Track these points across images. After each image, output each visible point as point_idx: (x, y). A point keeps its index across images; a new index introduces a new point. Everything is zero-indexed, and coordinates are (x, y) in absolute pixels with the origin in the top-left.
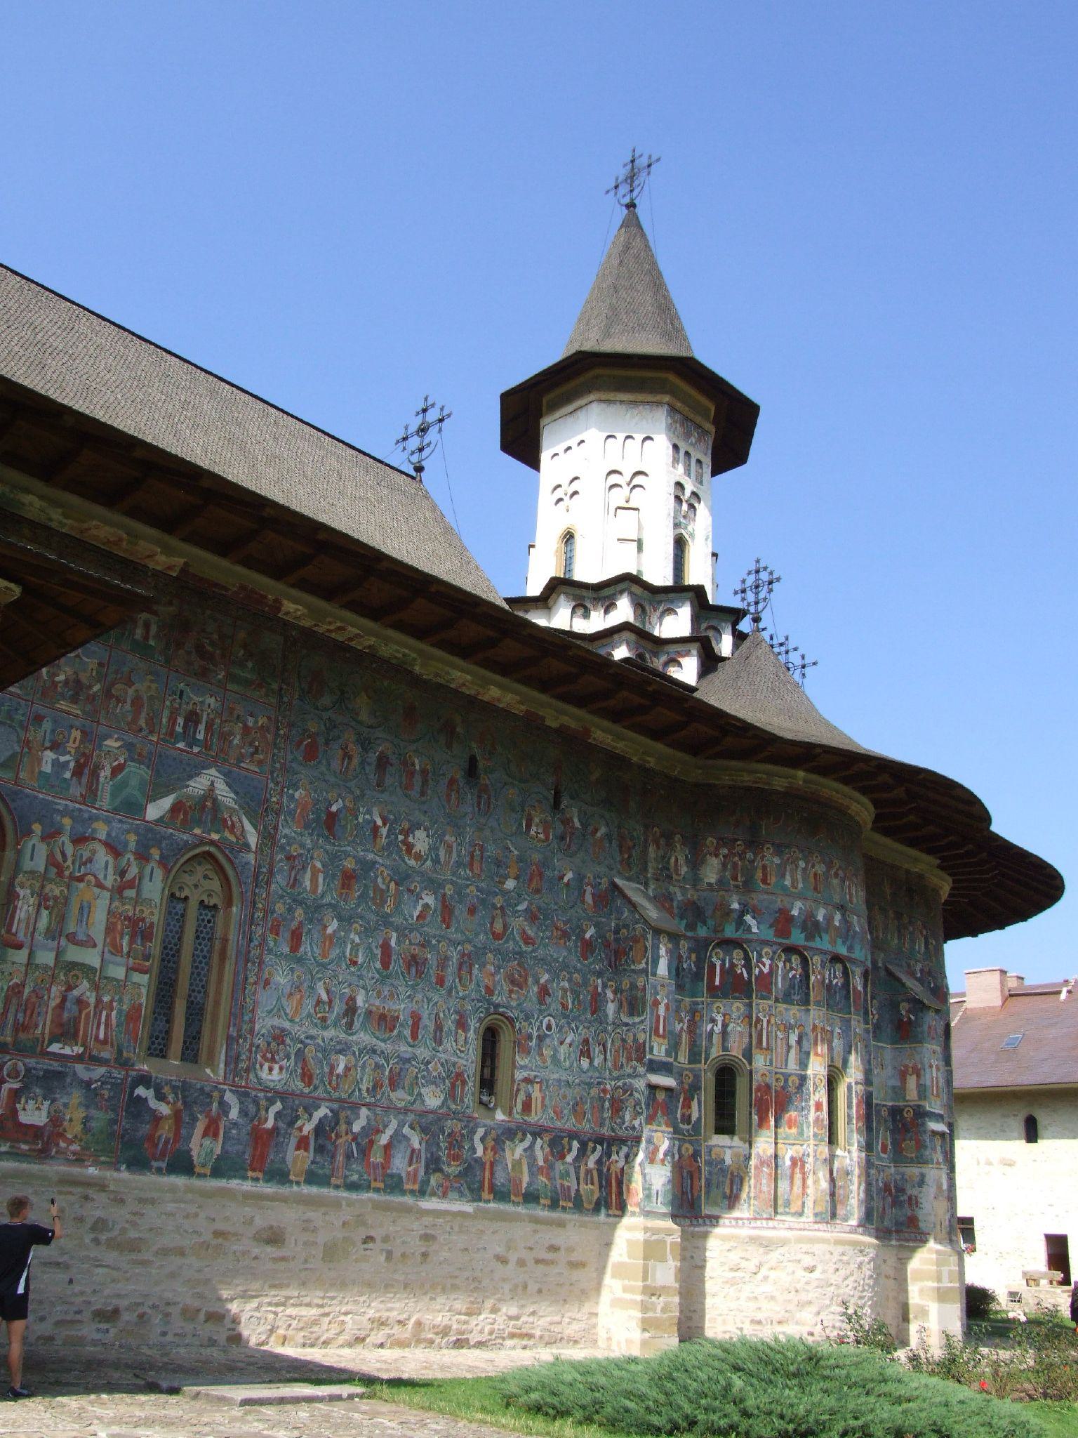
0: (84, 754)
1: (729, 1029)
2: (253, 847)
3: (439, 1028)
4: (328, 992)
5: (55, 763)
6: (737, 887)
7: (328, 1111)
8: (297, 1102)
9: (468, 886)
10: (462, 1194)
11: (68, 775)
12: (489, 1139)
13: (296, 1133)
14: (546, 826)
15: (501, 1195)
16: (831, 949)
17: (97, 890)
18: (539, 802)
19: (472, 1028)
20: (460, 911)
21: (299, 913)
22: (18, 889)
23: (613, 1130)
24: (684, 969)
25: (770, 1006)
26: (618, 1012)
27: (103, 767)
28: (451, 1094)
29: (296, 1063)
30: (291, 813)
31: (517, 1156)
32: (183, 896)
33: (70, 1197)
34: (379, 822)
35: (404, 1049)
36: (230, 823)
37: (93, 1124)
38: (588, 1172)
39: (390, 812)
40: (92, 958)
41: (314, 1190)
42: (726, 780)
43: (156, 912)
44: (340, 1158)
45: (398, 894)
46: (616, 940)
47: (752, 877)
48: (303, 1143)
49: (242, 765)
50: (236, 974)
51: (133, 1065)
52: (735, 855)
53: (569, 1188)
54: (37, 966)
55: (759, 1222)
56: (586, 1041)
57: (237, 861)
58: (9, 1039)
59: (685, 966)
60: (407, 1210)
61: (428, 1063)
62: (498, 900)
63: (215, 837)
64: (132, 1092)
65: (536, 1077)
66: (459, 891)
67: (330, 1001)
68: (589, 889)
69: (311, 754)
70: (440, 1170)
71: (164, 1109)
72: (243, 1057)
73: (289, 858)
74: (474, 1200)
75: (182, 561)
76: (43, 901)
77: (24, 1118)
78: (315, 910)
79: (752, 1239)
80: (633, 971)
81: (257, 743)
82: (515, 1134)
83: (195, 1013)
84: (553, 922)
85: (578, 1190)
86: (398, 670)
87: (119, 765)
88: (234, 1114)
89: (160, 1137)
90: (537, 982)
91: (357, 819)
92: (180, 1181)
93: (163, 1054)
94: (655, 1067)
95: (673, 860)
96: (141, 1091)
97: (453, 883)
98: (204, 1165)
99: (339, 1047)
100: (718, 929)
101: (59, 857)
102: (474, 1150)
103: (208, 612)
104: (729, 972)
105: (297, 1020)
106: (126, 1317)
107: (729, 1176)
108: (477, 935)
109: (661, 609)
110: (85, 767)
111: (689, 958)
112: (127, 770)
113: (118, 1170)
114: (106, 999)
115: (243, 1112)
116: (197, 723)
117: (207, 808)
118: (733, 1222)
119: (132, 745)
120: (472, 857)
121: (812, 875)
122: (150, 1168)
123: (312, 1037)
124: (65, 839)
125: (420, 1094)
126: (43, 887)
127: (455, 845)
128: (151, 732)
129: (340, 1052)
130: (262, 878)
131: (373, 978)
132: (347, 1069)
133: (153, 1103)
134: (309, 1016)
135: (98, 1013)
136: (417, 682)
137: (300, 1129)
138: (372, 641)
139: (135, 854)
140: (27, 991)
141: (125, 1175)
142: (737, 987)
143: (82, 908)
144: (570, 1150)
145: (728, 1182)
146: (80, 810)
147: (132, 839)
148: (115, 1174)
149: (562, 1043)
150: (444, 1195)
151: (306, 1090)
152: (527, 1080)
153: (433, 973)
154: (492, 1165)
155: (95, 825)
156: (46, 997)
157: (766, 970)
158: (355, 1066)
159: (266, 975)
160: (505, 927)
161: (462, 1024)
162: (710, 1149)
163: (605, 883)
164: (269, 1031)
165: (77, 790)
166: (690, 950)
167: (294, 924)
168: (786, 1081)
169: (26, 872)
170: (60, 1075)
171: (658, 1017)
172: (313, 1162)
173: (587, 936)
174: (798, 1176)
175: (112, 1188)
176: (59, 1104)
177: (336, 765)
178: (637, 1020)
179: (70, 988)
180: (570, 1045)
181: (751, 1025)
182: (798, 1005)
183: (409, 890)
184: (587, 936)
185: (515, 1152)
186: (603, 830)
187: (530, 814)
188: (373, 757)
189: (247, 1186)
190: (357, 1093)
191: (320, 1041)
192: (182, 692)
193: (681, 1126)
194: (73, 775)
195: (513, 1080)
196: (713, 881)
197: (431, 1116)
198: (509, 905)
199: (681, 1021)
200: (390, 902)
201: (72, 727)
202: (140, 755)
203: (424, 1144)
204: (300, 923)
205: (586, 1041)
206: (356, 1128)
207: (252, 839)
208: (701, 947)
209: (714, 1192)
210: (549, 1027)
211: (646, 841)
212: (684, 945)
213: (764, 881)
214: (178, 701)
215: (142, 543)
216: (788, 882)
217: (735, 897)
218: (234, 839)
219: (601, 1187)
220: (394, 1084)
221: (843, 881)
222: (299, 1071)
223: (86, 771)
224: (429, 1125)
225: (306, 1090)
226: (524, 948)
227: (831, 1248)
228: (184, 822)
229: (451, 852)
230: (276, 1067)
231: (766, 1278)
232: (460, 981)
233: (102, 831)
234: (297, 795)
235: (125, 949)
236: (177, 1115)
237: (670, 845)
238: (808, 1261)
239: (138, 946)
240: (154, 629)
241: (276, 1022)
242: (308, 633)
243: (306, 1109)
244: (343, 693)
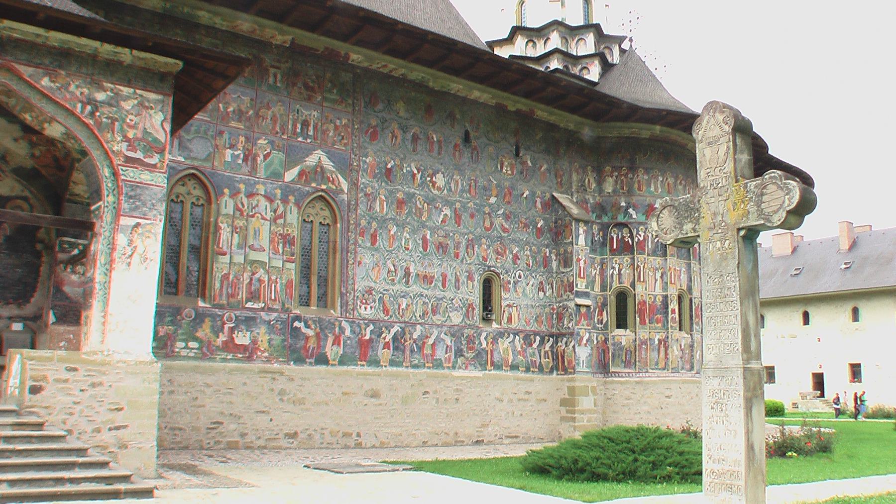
0: (248, 149)
1: (622, 272)
2: (346, 191)
3: (457, 280)
4: (394, 266)
5: (233, 155)
6: (624, 193)
7: (399, 328)
8: (381, 325)
9: (469, 202)
10: (476, 367)
11: (240, 161)
12: (489, 338)
13: (383, 341)
14: (512, 167)
15: (497, 366)
17: (263, 221)
18: (508, 153)
19: (476, 280)
20: (465, 217)
21: (374, 224)
22: (220, 224)
23: (558, 330)
25: (645, 259)
26: (558, 266)
27: (259, 156)
28: (467, 315)
29: (379, 304)
30: (365, 170)
31: (505, 346)
32: (310, 220)
33: (265, 379)
34: (416, 172)
35: (439, 293)
36: (331, 179)
37: (273, 342)
38: (546, 352)
39: (421, 165)
40: (263, 257)
41: (395, 369)
42: (615, 134)
43: (296, 230)
44: (408, 352)
45: (429, 210)
46: (555, 227)
47: (632, 187)
48: (386, 346)
49: (335, 146)
50: (342, 260)
51: (291, 311)
52: (621, 176)
53: (535, 361)
54: (235, 263)
55: (641, 374)
56: (541, 283)
57: (337, 199)
58: (225, 302)
59: (596, 239)
60: (445, 377)
61: (453, 299)
62: (487, 210)
63: (324, 187)
64: (292, 325)
66: (464, 206)
67: (396, 271)
68: (539, 200)
69: (374, 137)
70: (463, 356)
71: (310, 333)
72: (350, 303)
73: (366, 195)
74: (482, 370)
75: (290, 37)
76: (234, 230)
77: (238, 341)
78: (383, 222)
79: (637, 383)
80: (565, 243)
81: (342, 134)
82: (504, 335)
83: (324, 282)
84: (519, 219)
85: (540, 362)
86: (420, 86)
87: (268, 153)
88: (348, 333)
89: (309, 346)
90: (512, 252)
91: (402, 171)
92: (322, 368)
93: (308, 304)
94: (579, 294)
95: (587, 180)
96: (296, 324)
97: (460, 201)
98: (334, 360)
99: (402, 294)
100: (614, 217)
101: (240, 206)
102: (481, 344)
103: (309, 65)
104: (621, 241)
105: (378, 282)
106: (301, 436)
107: (624, 351)
109: (576, 39)
110: (249, 157)
111: (599, 234)
112: (271, 157)
113: (289, 365)
114: (273, 278)
115: (353, 332)
116: (308, 125)
117: (319, 172)
118: (627, 375)
119: (273, 141)
120: (470, 186)
121: (666, 184)
122: (306, 363)
123: (387, 290)
124: (242, 195)
125: (449, 316)
126: (233, 222)
127: (460, 181)
128: (283, 134)
129: (403, 297)
130: (352, 207)
131: (418, 256)
132: (408, 305)
133: (304, 330)
134: (384, 279)
135: (270, 286)
136: (431, 92)
137: (384, 338)
138: (403, 71)
139: (281, 200)
140: (231, 277)
141: (292, 366)
142: (626, 248)
143: (255, 231)
144: (535, 341)
145: (624, 353)
146: (249, 179)
147: (278, 192)
148: (288, 367)
150: (466, 368)
151: (386, 318)
152: (509, 306)
153: (452, 251)
154: (492, 352)
155: (258, 187)
156: (242, 279)
157: (641, 239)
158: (412, 303)
159: (359, 259)
160: (492, 224)
161: (470, 278)
162: (614, 337)
163: (548, 195)
164: (363, 289)
165: (246, 169)
166: (600, 230)
167: (372, 231)
168: (655, 299)
169: (224, 215)
170: (253, 319)
171: (580, 267)
172: (393, 355)
173: (539, 226)
174: (662, 349)
175: (286, 373)
176: (254, 334)
177: (388, 141)
178: (569, 270)
179: (253, 274)
180: (532, 286)
181: (634, 270)
182: (660, 257)
183: (436, 208)
184: (539, 226)
185: (504, 344)
187: (502, 160)
188: (409, 136)
189: (358, 369)
190: (414, 318)
191: (391, 291)
192: (298, 110)
193: (598, 325)
194: (243, 161)
195: (501, 307)
196: (610, 191)
197: (456, 327)
198: (492, 212)
199: (595, 269)
200: (425, 214)
201: (239, 135)
202: (278, 146)
203: (453, 342)
204: (375, 229)
205: (541, 283)
206: (415, 336)
207: (345, 186)
208: (604, 228)
209: (617, 359)
210: (520, 277)
211: (571, 171)
212: (595, 228)
213: (639, 189)
214: (296, 115)
215: (268, 30)
216: (652, 189)
217: (623, 199)
218: (334, 187)
219: (553, 359)
220: (434, 312)
221: (685, 186)
222: (382, 308)
223: (250, 158)
224: (456, 333)
225: (386, 318)
228: (306, 180)
229: (458, 185)
230: (369, 307)
231: (645, 402)
232: (468, 254)
233: (261, 189)
234: (368, 161)
235: (281, 251)
236: (317, 335)
237: (585, 172)
238: (668, 393)
239: (288, 249)
240: (279, 77)
241: (366, 283)
242: (366, 70)
243: (386, 328)
244: (389, 101)
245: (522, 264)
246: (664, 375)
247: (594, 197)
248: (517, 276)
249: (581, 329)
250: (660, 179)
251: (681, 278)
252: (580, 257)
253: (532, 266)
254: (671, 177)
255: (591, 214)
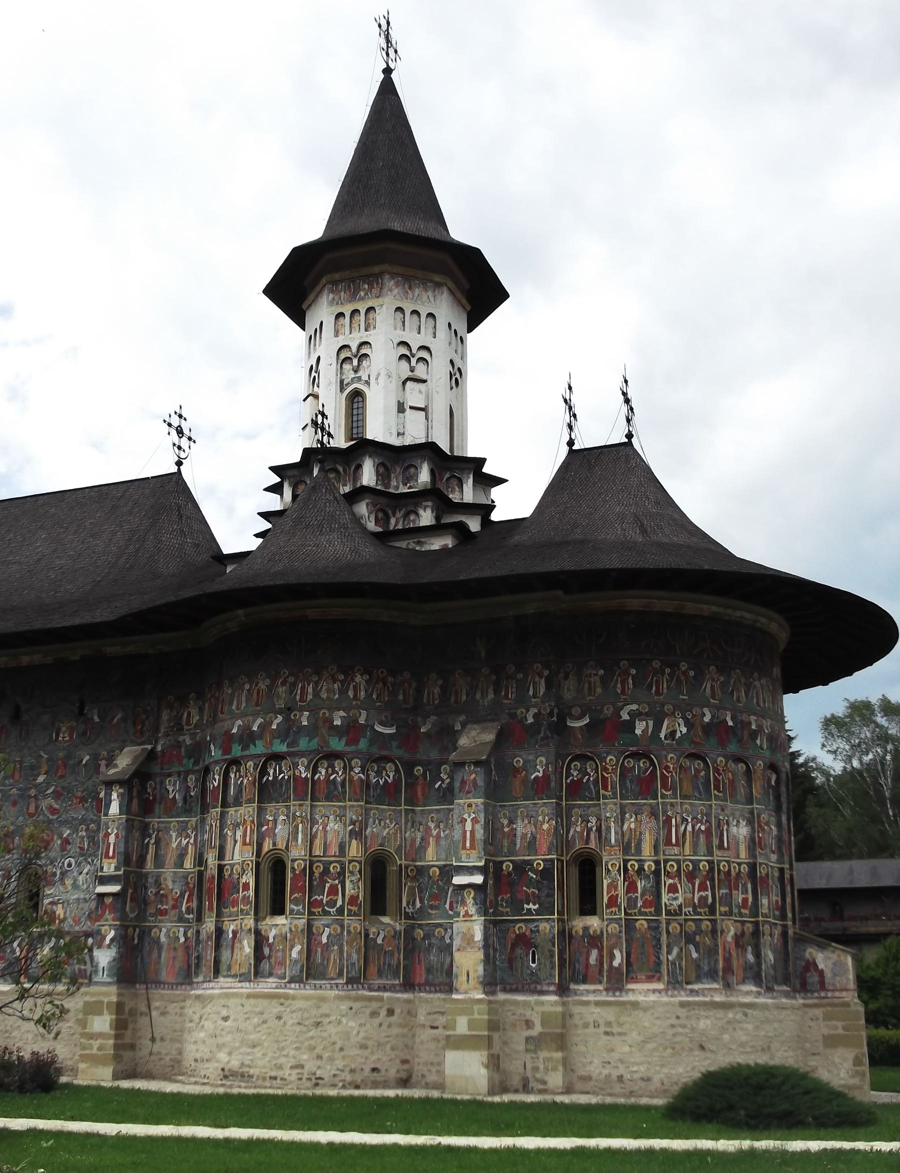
16: (265, 751)
24: (191, 796)
53: (85, 970)
59: (192, 794)
65: (59, 900)
90: (60, 836)
95: (186, 714)
102: (14, 952)
108: (17, 818)
121: (255, 692)
149: (81, 873)
157: (216, 784)
160: (37, 808)
168: (232, 870)
180: (87, 874)
186: (119, 716)
193: (187, 916)
198: (40, 793)
199: (188, 836)
210: (70, 865)
213: (222, 713)
216: (234, 707)
221: (294, 685)
226: (51, 817)
227: (244, 1001)
238: (224, 1013)
245: (73, 849)
246: (229, 985)
247: (193, 736)
248: (66, 865)
249: (103, 925)
250: (247, 687)
251: (277, 831)
252: (109, 831)
253: (88, 850)
254: (263, 680)
255: (185, 761)
